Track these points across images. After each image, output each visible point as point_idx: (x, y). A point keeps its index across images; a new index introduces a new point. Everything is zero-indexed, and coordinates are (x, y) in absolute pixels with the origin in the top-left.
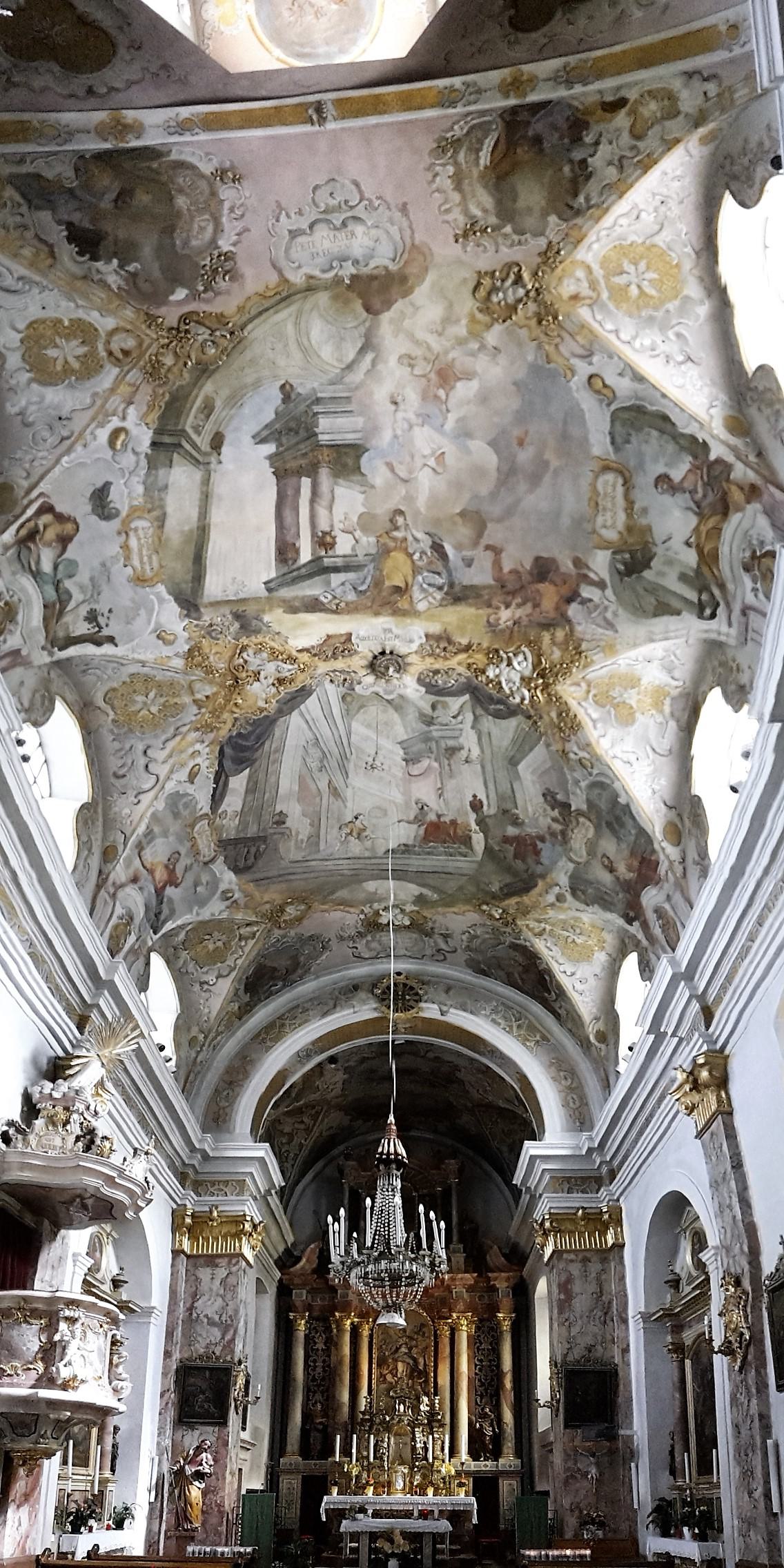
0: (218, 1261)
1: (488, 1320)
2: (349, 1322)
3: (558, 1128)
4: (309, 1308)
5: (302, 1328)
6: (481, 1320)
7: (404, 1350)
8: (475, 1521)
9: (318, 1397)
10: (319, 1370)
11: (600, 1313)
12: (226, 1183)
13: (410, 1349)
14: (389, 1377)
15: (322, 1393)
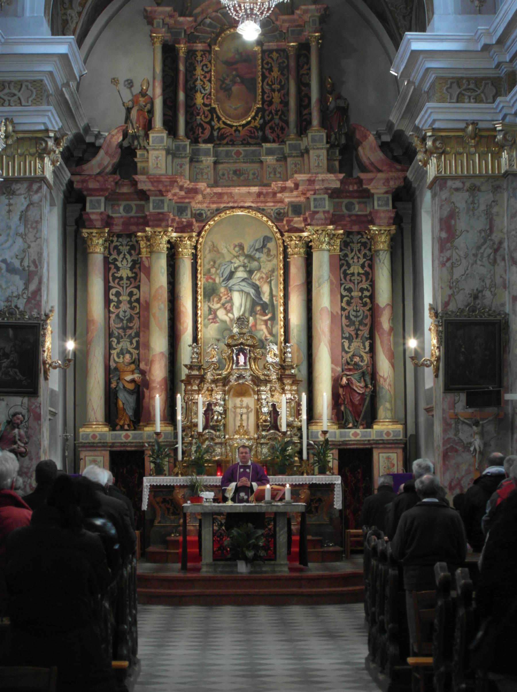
0: (14, 187)
1: (359, 233)
2: (165, 238)
3: (451, 9)
4: (108, 222)
5: (100, 249)
6: (348, 234)
7: (241, 274)
8: (338, 504)
9: (125, 344)
10: (125, 306)
11: (489, 251)
12: (19, 84)
13: (250, 272)
14: (221, 314)
15: (131, 338)
